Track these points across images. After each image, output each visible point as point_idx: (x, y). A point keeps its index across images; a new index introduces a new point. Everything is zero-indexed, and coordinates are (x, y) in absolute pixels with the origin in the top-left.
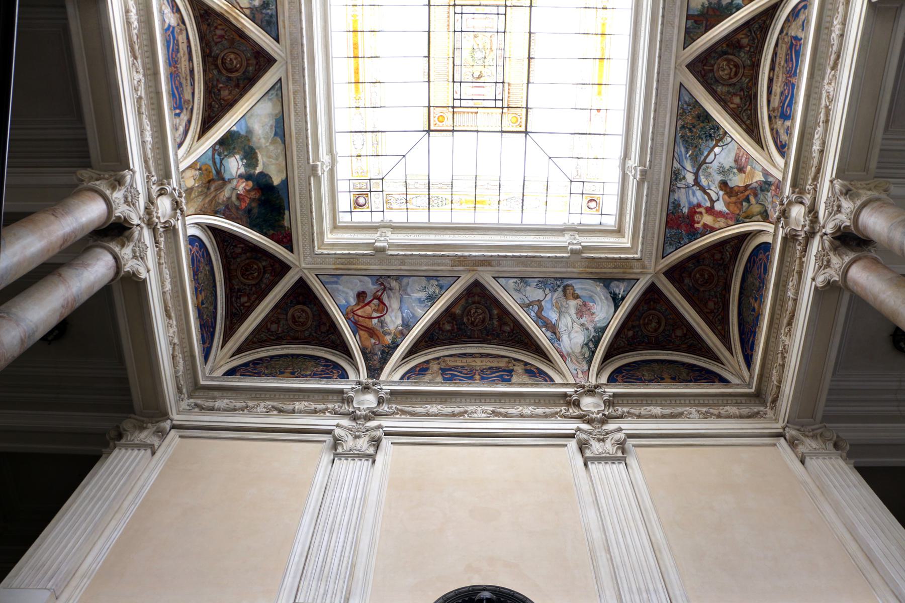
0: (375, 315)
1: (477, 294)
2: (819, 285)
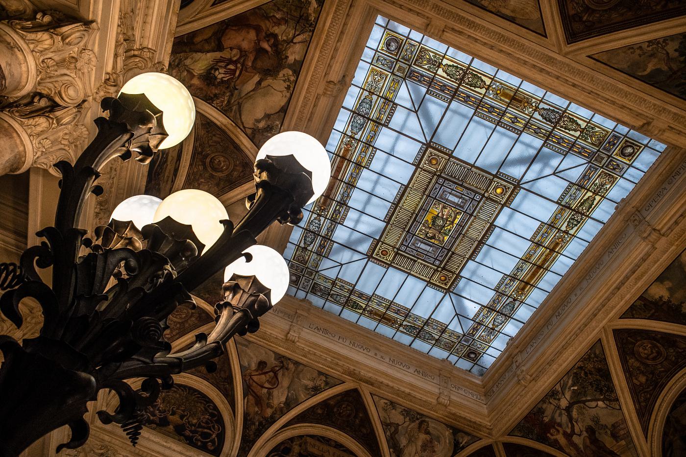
0: (267, 385)
1: (353, 397)
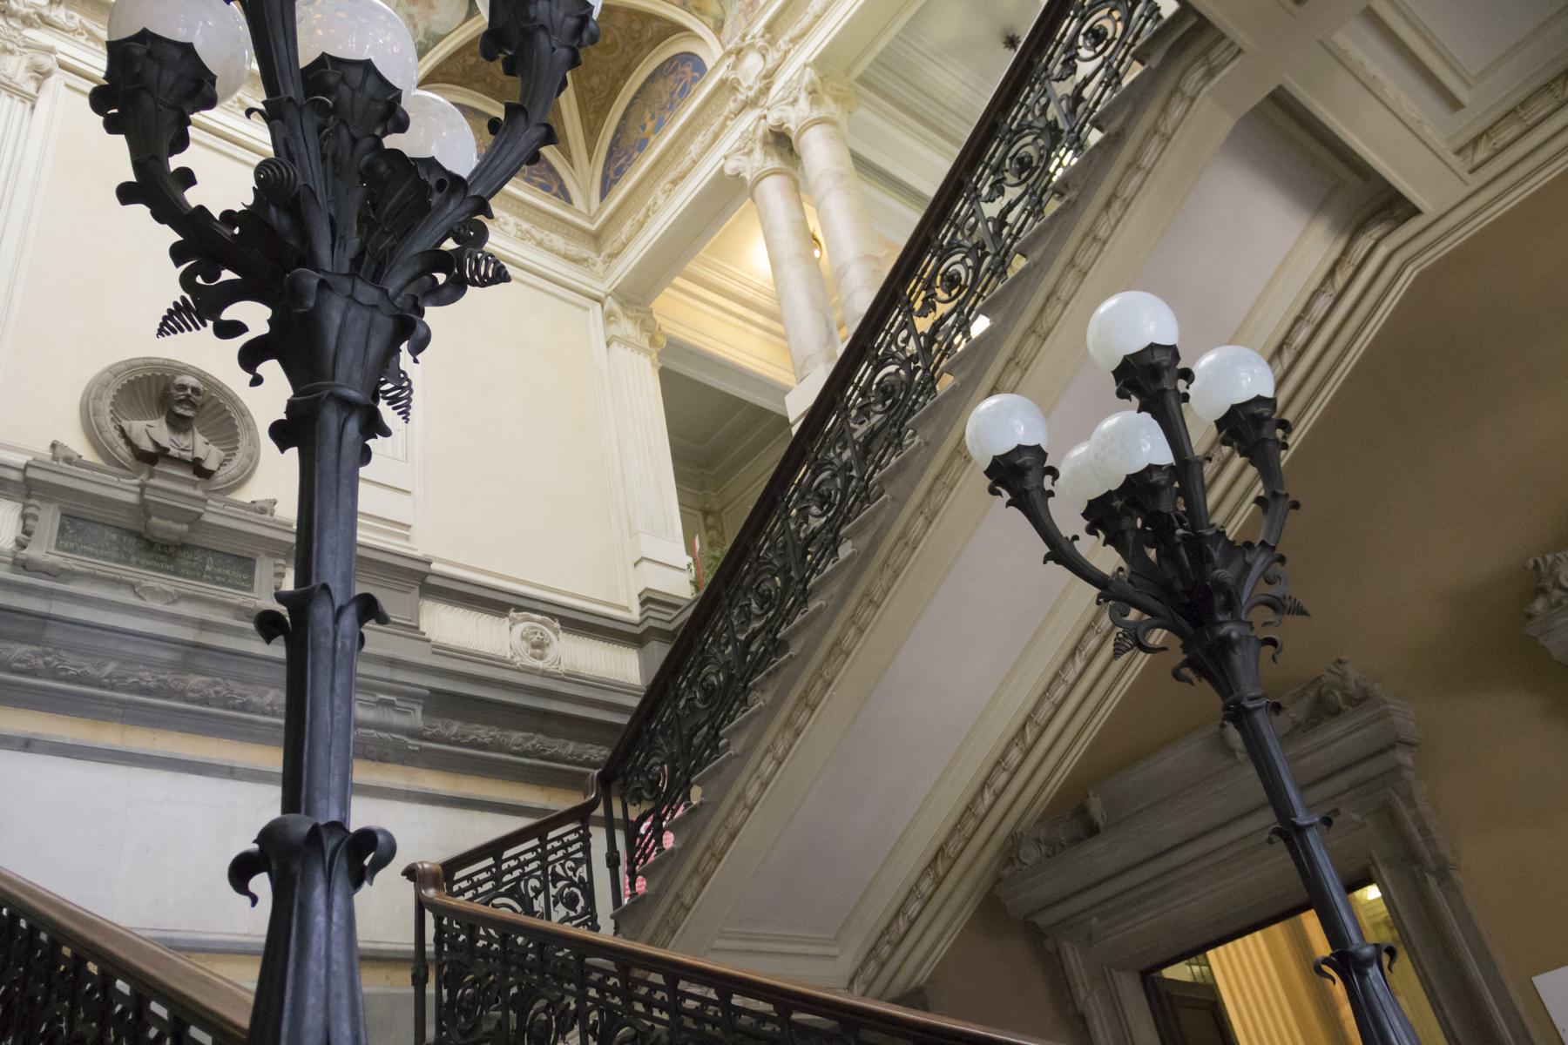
2: (728, 171)
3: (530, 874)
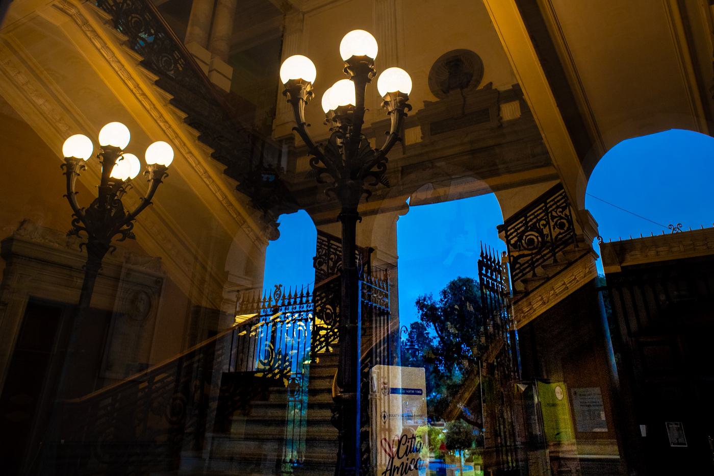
3: (541, 219)
